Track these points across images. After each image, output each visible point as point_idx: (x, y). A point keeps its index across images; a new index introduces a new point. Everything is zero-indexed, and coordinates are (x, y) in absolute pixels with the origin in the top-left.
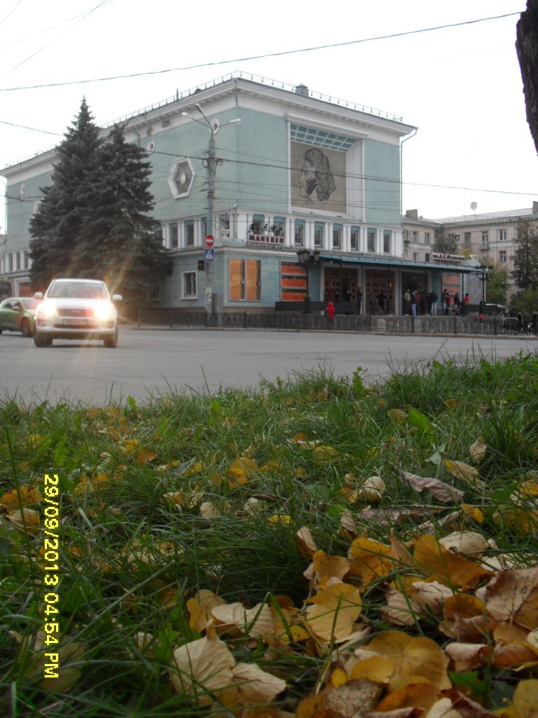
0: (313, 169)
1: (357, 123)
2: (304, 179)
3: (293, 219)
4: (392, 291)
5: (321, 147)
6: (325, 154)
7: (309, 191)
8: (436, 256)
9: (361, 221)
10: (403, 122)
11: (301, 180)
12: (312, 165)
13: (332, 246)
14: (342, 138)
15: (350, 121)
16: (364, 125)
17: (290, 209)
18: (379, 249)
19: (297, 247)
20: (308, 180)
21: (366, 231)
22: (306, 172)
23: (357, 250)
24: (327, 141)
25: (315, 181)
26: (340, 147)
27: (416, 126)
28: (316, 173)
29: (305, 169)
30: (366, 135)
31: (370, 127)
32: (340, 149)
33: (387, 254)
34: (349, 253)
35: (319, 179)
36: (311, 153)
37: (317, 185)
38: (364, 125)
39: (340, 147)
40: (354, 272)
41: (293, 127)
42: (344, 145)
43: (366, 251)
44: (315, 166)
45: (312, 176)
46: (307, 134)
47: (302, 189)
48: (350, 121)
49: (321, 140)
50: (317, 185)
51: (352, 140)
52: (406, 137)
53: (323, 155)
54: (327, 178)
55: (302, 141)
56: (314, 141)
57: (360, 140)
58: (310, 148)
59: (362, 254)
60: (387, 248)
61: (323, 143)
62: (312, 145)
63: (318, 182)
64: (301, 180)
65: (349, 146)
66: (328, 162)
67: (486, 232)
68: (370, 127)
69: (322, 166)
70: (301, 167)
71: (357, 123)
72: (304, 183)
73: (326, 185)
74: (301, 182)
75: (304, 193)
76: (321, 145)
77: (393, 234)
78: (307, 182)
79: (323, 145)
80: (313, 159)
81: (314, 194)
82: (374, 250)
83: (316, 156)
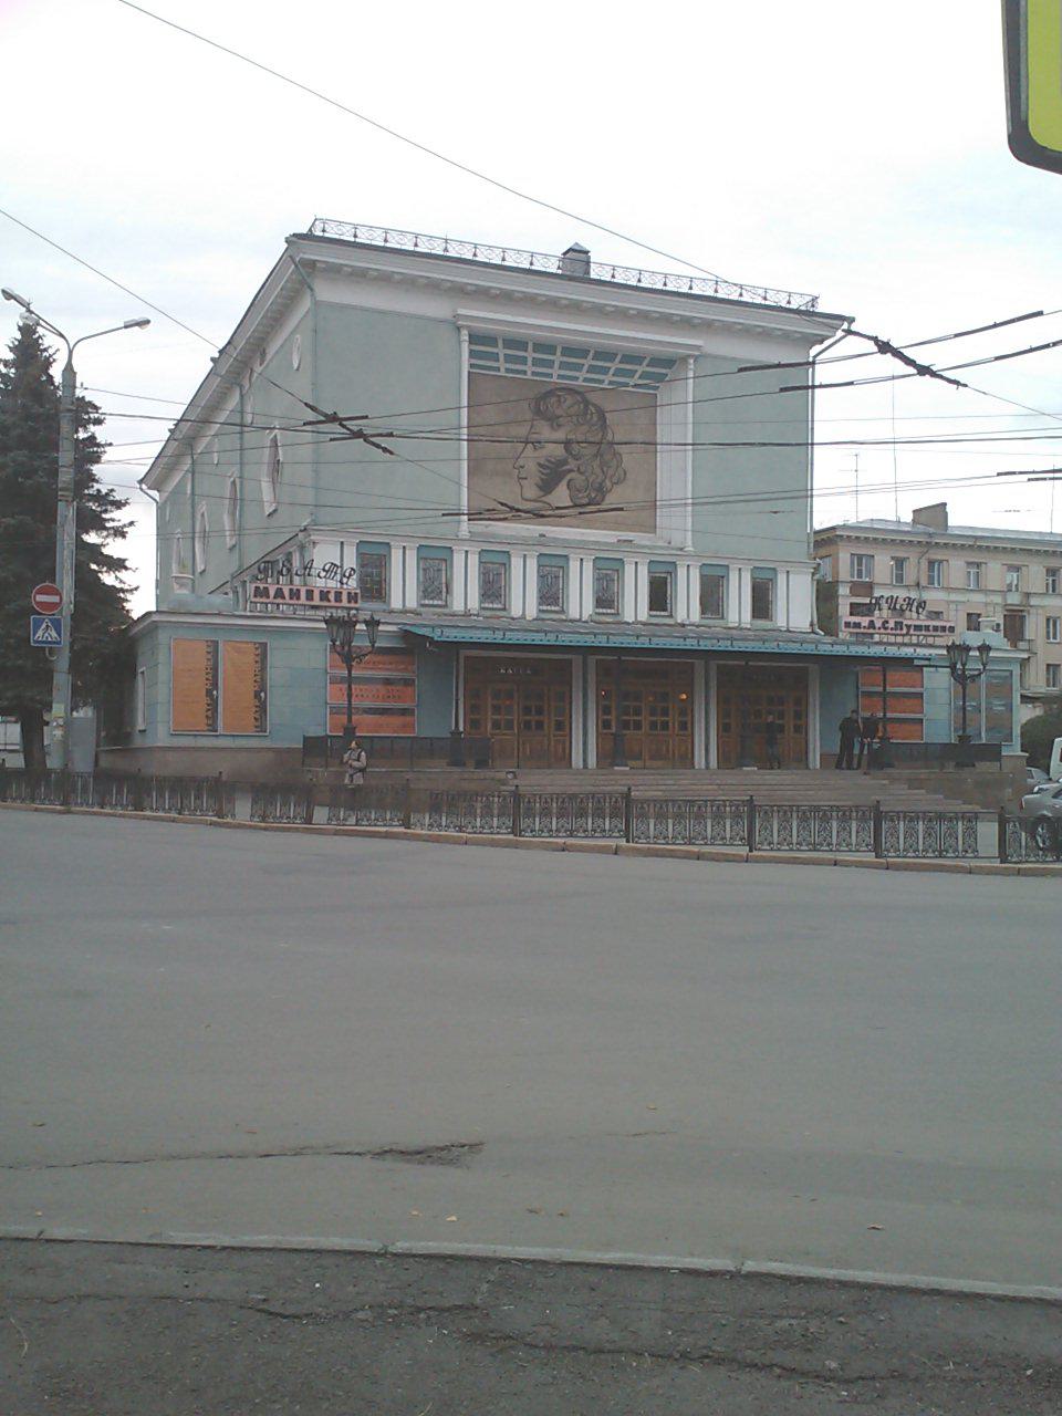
0: (560, 435)
1: (667, 321)
2: (531, 459)
3: (474, 549)
4: (686, 711)
5: (580, 382)
6: (591, 397)
7: (547, 486)
8: (857, 625)
9: (681, 549)
10: (821, 308)
11: (521, 462)
12: (554, 422)
13: (589, 608)
14: (633, 358)
15: (644, 318)
16: (687, 324)
17: (465, 527)
18: (738, 609)
19: (488, 613)
21: (695, 575)
22: (537, 444)
23: (671, 616)
24: (592, 369)
25: (565, 462)
26: (636, 380)
27: (846, 314)
28: (567, 444)
30: (698, 348)
31: (707, 326)
32: (636, 386)
33: (761, 623)
34: (644, 624)
35: (576, 458)
36: (554, 399)
37: (571, 471)
38: (687, 324)
39: (636, 380)
40: (563, 669)
42: (644, 376)
43: (696, 616)
45: (558, 451)
46: (530, 355)
47: (523, 482)
48: (644, 318)
49: (579, 367)
50: (571, 471)
51: (669, 362)
52: (827, 343)
53: (587, 403)
54: (598, 454)
55: (525, 373)
56: (555, 371)
57: (684, 359)
59: (683, 625)
60: (762, 606)
61: (583, 375)
62: (555, 379)
63: (572, 464)
64: (521, 462)
65: (661, 378)
66: (601, 414)
67: (978, 565)
68: (707, 326)
69: (585, 428)
70: (522, 431)
71: (667, 321)
72: (531, 467)
73: (598, 471)
74: (522, 467)
75: (531, 491)
76: (581, 379)
77: (781, 579)
78: (539, 464)
79: (585, 380)
82: (723, 618)
83: (565, 406)
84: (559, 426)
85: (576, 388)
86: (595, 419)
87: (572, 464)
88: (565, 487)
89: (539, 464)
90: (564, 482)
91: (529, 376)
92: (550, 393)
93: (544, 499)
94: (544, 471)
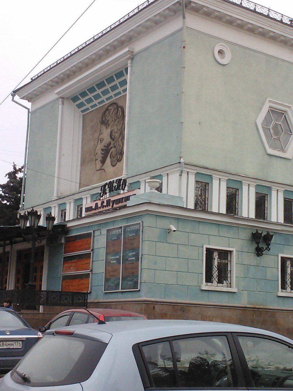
0: (109, 131)
5: (114, 98)
20: (103, 148)
29: (101, 136)
35: (113, 140)
41: (75, 99)
44: (110, 127)
47: (97, 162)
50: (112, 147)
53: (118, 107)
58: (106, 107)
62: (107, 102)
74: (96, 154)
75: (99, 165)
80: (108, 119)
81: (108, 160)
84: (108, 126)
85: (112, 102)
86: (120, 114)
87: (112, 142)
88: (109, 157)
89: (102, 150)
90: (109, 155)
91: (99, 106)
92: (107, 109)
93: (103, 168)
94: (103, 152)
